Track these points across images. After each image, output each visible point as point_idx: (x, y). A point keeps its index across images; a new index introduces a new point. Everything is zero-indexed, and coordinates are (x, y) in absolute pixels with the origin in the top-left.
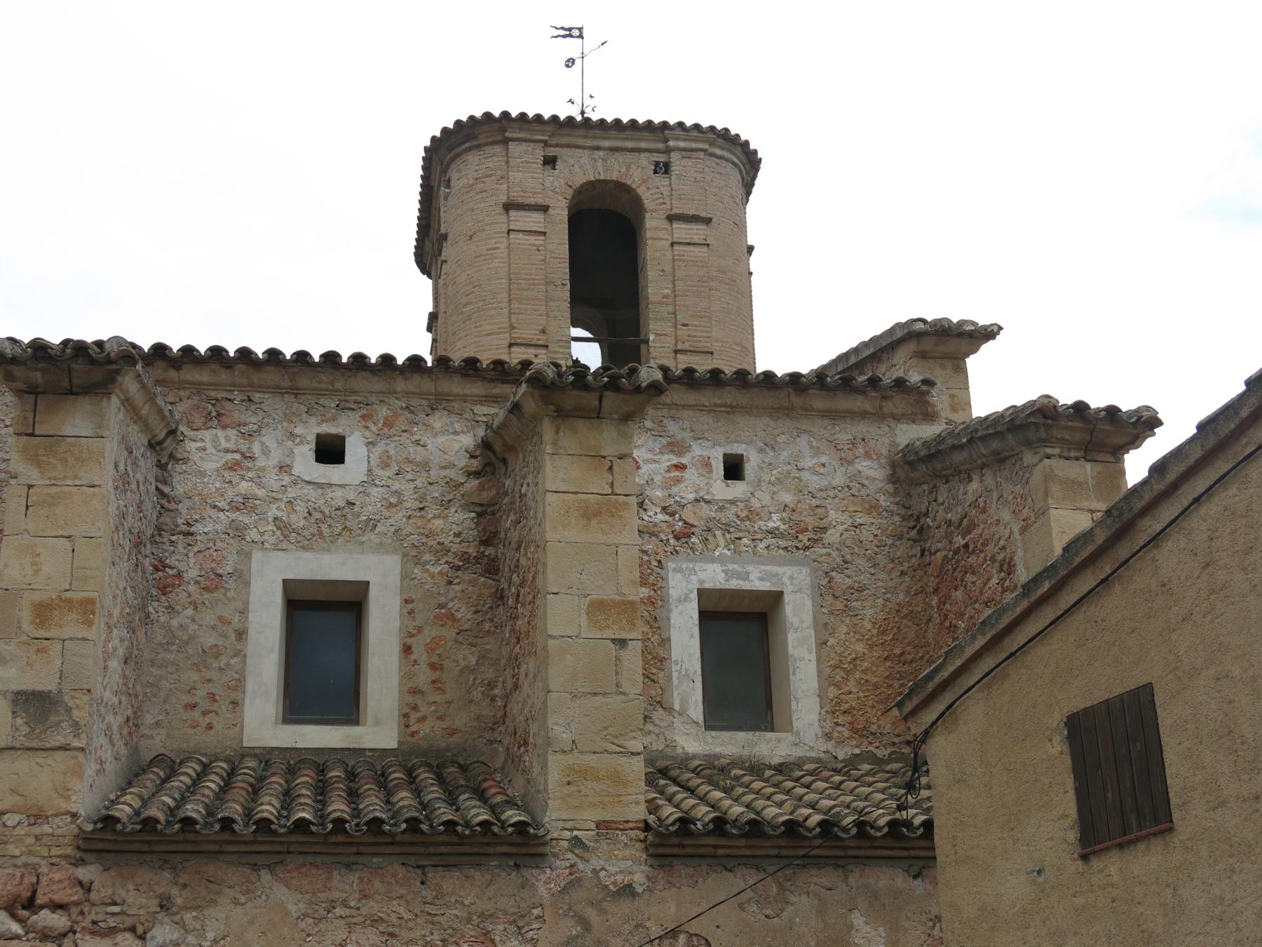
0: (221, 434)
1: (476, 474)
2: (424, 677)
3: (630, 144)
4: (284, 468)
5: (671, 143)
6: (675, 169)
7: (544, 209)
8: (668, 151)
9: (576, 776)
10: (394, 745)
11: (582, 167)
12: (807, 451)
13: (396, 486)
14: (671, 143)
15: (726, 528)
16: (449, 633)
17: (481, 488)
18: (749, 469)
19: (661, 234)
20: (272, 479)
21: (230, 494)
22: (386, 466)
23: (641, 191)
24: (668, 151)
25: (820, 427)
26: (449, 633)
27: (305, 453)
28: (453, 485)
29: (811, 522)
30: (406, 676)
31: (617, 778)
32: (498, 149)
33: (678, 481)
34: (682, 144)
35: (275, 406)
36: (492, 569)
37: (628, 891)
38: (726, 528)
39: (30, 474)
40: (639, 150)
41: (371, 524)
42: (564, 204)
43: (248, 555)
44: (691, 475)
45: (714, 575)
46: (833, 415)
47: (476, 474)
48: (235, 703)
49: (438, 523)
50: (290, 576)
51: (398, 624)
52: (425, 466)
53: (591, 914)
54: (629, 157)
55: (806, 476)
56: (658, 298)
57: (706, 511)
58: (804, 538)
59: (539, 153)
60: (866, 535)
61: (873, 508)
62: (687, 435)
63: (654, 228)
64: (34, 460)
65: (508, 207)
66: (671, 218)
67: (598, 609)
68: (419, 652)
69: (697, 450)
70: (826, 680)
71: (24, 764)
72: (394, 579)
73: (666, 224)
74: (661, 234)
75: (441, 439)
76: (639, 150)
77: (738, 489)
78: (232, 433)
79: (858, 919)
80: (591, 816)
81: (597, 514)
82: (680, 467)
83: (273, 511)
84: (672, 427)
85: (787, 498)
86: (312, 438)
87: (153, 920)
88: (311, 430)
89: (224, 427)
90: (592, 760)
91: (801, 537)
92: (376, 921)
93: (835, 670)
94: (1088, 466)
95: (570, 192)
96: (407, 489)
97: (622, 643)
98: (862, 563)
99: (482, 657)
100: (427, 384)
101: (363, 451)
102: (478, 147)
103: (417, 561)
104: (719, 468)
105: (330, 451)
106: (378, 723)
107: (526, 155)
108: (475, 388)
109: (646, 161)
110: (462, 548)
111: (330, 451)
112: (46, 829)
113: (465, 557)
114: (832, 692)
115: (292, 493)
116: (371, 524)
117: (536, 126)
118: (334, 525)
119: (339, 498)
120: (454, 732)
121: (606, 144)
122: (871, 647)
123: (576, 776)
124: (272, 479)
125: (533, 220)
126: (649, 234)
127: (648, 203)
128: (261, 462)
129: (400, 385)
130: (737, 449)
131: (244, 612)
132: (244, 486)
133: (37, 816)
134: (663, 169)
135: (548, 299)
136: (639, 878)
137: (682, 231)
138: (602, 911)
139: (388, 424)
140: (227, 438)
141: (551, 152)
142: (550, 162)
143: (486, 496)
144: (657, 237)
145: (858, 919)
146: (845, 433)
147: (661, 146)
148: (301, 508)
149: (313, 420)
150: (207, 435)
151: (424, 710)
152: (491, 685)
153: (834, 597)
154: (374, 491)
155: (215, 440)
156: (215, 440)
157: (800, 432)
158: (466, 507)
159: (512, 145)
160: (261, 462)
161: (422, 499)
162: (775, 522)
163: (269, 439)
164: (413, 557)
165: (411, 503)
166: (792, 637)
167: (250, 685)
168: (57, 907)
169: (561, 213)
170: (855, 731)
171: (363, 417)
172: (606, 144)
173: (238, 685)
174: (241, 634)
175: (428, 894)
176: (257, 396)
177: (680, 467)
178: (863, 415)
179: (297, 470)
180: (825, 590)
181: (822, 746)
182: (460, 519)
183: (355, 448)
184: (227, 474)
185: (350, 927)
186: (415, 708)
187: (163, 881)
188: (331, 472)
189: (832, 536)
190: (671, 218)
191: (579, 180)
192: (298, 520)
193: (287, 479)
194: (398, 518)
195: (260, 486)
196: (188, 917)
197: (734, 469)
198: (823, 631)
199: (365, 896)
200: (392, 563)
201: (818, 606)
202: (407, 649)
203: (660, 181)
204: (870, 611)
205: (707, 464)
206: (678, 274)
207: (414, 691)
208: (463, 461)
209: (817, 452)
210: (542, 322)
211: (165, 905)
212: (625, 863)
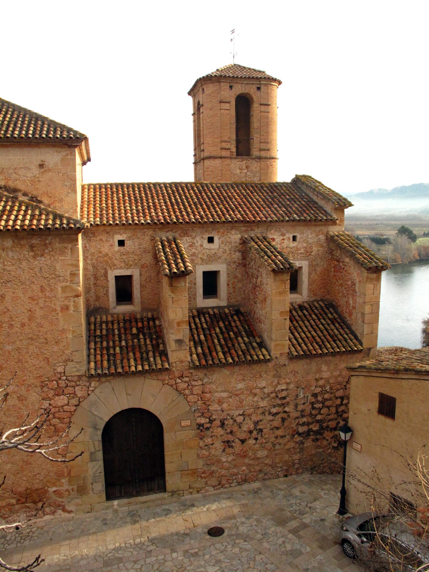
0: (187, 238)
1: (241, 244)
2: (231, 290)
3: (251, 82)
4: (202, 246)
5: (262, 82)
6: (262, 90)
7: (229, 102)
8: (260, 84)
9: (276, 345)
10: (226, 305)
11: (239, 89)
12: (310, 234)
13: (225, 248)
14: (262, 82)
15: (292, 253)
16: (236, 280)
17: (242, 247)
18: (298, 239)
19: (258, 109)
20: (199, 248)
21: (191, 253)
22: (223, 243)
23: (253, 96)
24: (260, 84)
25: (313, 229)
26: (236, 280)
27: (206, 241)
28: (236, 247)
29: (309, 250)
30: (228, 290)
31: (284, 345)
32: (218, 84)
33: (283, 243)
34: (264, 83)
35: (198, 231)
36: (245, 266)
37: (285, 365)
38: (292, 253)
39: (172, 295)
40: (253, 84)
41: (220, 258)
42: (234, 100)
43: (195, 266)
44: (286, 241)
46: (316, 225)
47: (241, 244)
48: (195, 299)
49: (234, 256)
50: (204, 270)
51: (226, 279)
52: (230, 243)
53: (278, 369)
54: (251, 86)
55: (309, 239)
56: (256, 127)
57: (289, 249)
58: (308, 254)
59: (228, 85)
60: (320, 253)
61: (322, 246)
62: (285, 232)
64: (173, 292)
65: (221, 102)
66: (261, 105)
67: (282, 313)
68: (230, 285)
69: (287, 235)
70: (310, 285)
71: (178, 353)
72: (225, 270)
73: (259, 106)
74: (258, 109)
75: (234, 236)
76: (253, 84)
77: (295, 244)
78: (190, 238)
79: (323, 366)
80: (279, 352)
81: (282, 293)
82: (284, 239)
83: (200, 256)
84: (282, 230)
85: (305, 245)
86: (207, 238)
87: (204, 378)
88: (206, 236)
89: (188, 236)
90: (279, 342)
91: (307, 254)
92: (241, 374)
94: (375, 275)
95: (236, 97)
96: (227, 248)
97: (286, 319)
98: (318, 259)
99: (243, 285)
100: (231, 225)
101: (218, 240)
102: (212, 83)
103: (230, 265)
104: (291, 239)
105: (211, 240)
106: (223, 300)
108: (241, 225)
109: (255, 87)
110: (239, 261)
111: (211, 240)
112: (184, 364)
113: (239, 264)
114: (310, 287)
115: (203, 251)
116: (220, 258)
117: (228, 79)
118: (213, 258)
119: (213, 252)
120: (237, 301)
121: (245, 82)
122: (319, 277)
123: (276, 345)
124: (199, 248)
125: (227, 106)
126: (255, 109)
127: (255, 99)
128: (197, 244)
129: (226, 225)
130: (295, 234)
131: (195, 279)
132: (193, 250)
133: (182, 362)
134: (259, 89)
135: (230, 128)
136: (287, 363)
137: (263, 108)
138: (280, 369)
139: (223, 233)
140: (189, 239)
141: (231, 84)
142: (231, 87)
143: (244, 248)
144: (255, 107)
145: (323, 366)
146: (318, 229)
147: (259, 83)
148: (206, 255)
149: (207, 234)
150: (184, 238)
151: (232, 297)
152: (245, 291)
153: (312, 266)
154: (221, 250)
155: (186, 240)
156: (186, 240)
157: (309, 229)
158: (239, 251)
159: (222, 84)
160: (197, 244)
161: (230, 251)
162: (302, 251)
163: (198, 239)
165: (228, 252)
166: (304, 276)
167: (198, 294)
168: (186, 377)
169: (233, 103)
170: (314, 294)
171: (218, 232)
172: (245, 82)
173: (195, 295)
174: (195, 284)
175: (251, 369)
176: (195, 229)
177: (284, 239)
178: (322, 225)
179: (205, 246)
181: (308, 299)
183: (216, 239)
184: (190, 248)
185: (237, 375)
186: (230, 297)
187: (205, 371)
188: (211, 246)
189: (313, 254)
190: (261, 105)
191: (238, 93)
192: (205, 258)
193: (202, 248)
194: (225, 256)
195: (197, 250)
196: (210, 377)
197: (294, 238)
198: (310, 274)
199: (240, 370)
201: (309, 269)
202: (228, 285)
203: (258, 93)
204: (319, 269)
205: (289, 238)
206: (262, 121)
207: (230, 293)
208: (238, 241)
209: (312, 234)
210: (229, 135)
211: (205, 375)
212: (284, 360)
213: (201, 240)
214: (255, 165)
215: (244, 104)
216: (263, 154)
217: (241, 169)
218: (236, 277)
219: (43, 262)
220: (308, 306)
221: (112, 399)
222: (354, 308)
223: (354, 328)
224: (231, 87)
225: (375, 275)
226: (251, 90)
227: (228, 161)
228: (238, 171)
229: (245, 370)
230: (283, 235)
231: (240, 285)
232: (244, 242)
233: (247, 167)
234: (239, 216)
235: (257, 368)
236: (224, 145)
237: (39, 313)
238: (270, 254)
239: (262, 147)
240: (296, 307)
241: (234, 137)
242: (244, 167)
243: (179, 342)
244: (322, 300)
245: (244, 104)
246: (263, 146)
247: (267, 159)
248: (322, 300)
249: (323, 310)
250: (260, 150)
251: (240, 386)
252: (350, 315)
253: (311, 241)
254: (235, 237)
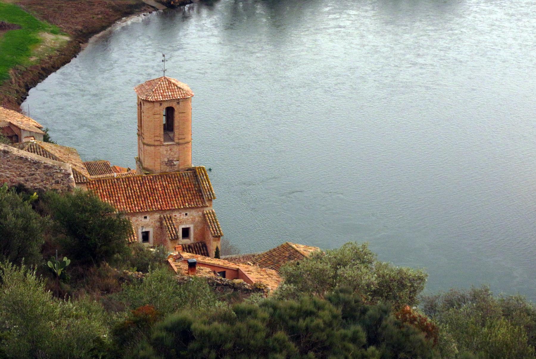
2: (155, 239)
11: (166, 105)
36: (162, 228)
45: (184, 227)
63: (176, 113)
77: (187, 217)
88: (143, 216)
91: (193, 221)
93: (195, 234)
105: (145, 217)
107: (157, 105)
124: (140, 222)
127: (176, 110)
137: (181, 115)
146: (198, 210)
153: (195, 227)
164: (154, 228)
180: (194, 227)
182: (159, 223)
183: (148, 218)
197: (186, 214)
198: (194, 230)
200: (152, 229)
203: (178, 106)
204: (199, 228)
213: (141, 218)
214: (176, 148)
215: (170, 111)
216: (181, 141)
217: (167, 151)
218: (157, 233)
220: (193, 246)
224: (161, 104)
225: (217, 238)
226: (174, 105)
227: (158, 148)
228: (165, 152)
230: (180, 213)
231: (159, 237)
233: (170, 150)
234: (159, 206)
236: (157, 138)
238: (170, 229)
239: (180, 138)
240: (187, 246)
241: (162, 133)
242: (169, 150)
244: (201, 242)
245: (170, 111)
246: (181, 137)
247: (183, 144)
248: (201, 242)
249: (200, 248)
250: (179, 139)
253: (195, 215)
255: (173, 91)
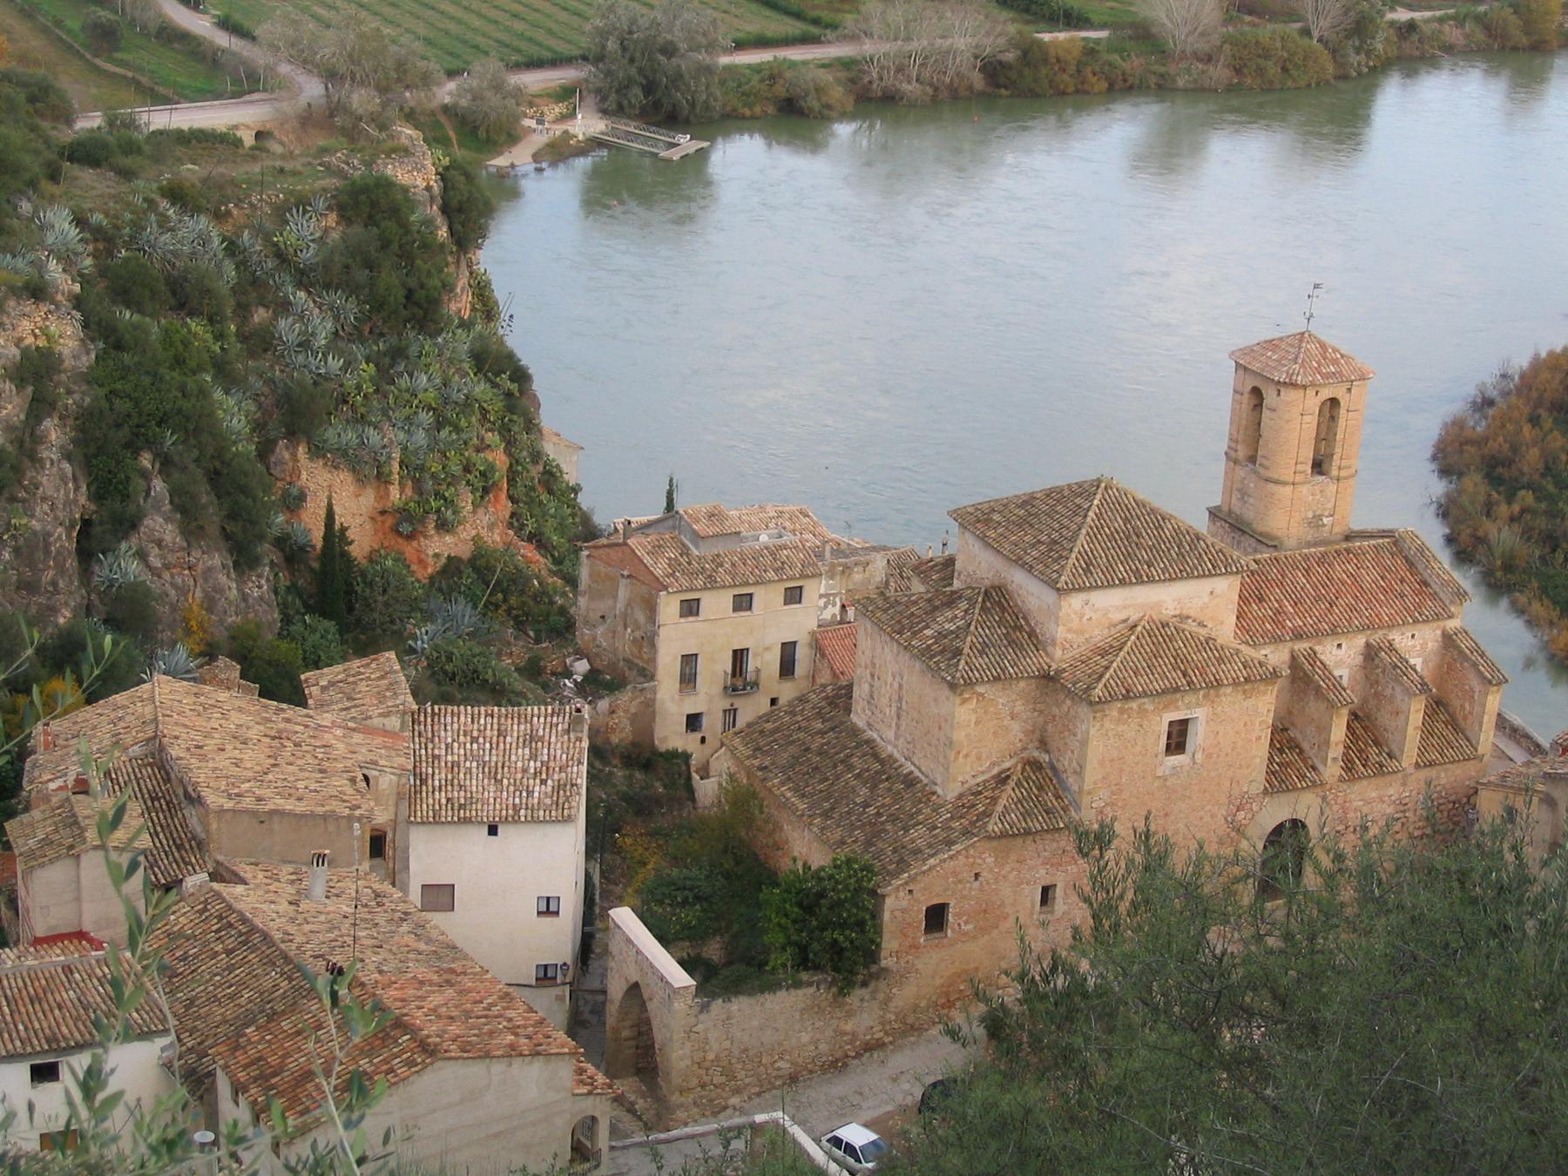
11: (1326, 394)
105: (1339, 646)
134: (1349, 390)
153: (1425, 662)
212: (1411, 770)
216: (1343, 473)
219: (1251, 702)
221: (1276, 812)
222: (1471, 713)
223: (1468, 733)
229: (1380, 781)
232: (1368, 645)
235: (1389, 778)
237: (1240, 743)
243: (1334, 759)
251: (1374, 794)
252: (1465, 719)
254: (1361, 641)
255: (1335, 362)
